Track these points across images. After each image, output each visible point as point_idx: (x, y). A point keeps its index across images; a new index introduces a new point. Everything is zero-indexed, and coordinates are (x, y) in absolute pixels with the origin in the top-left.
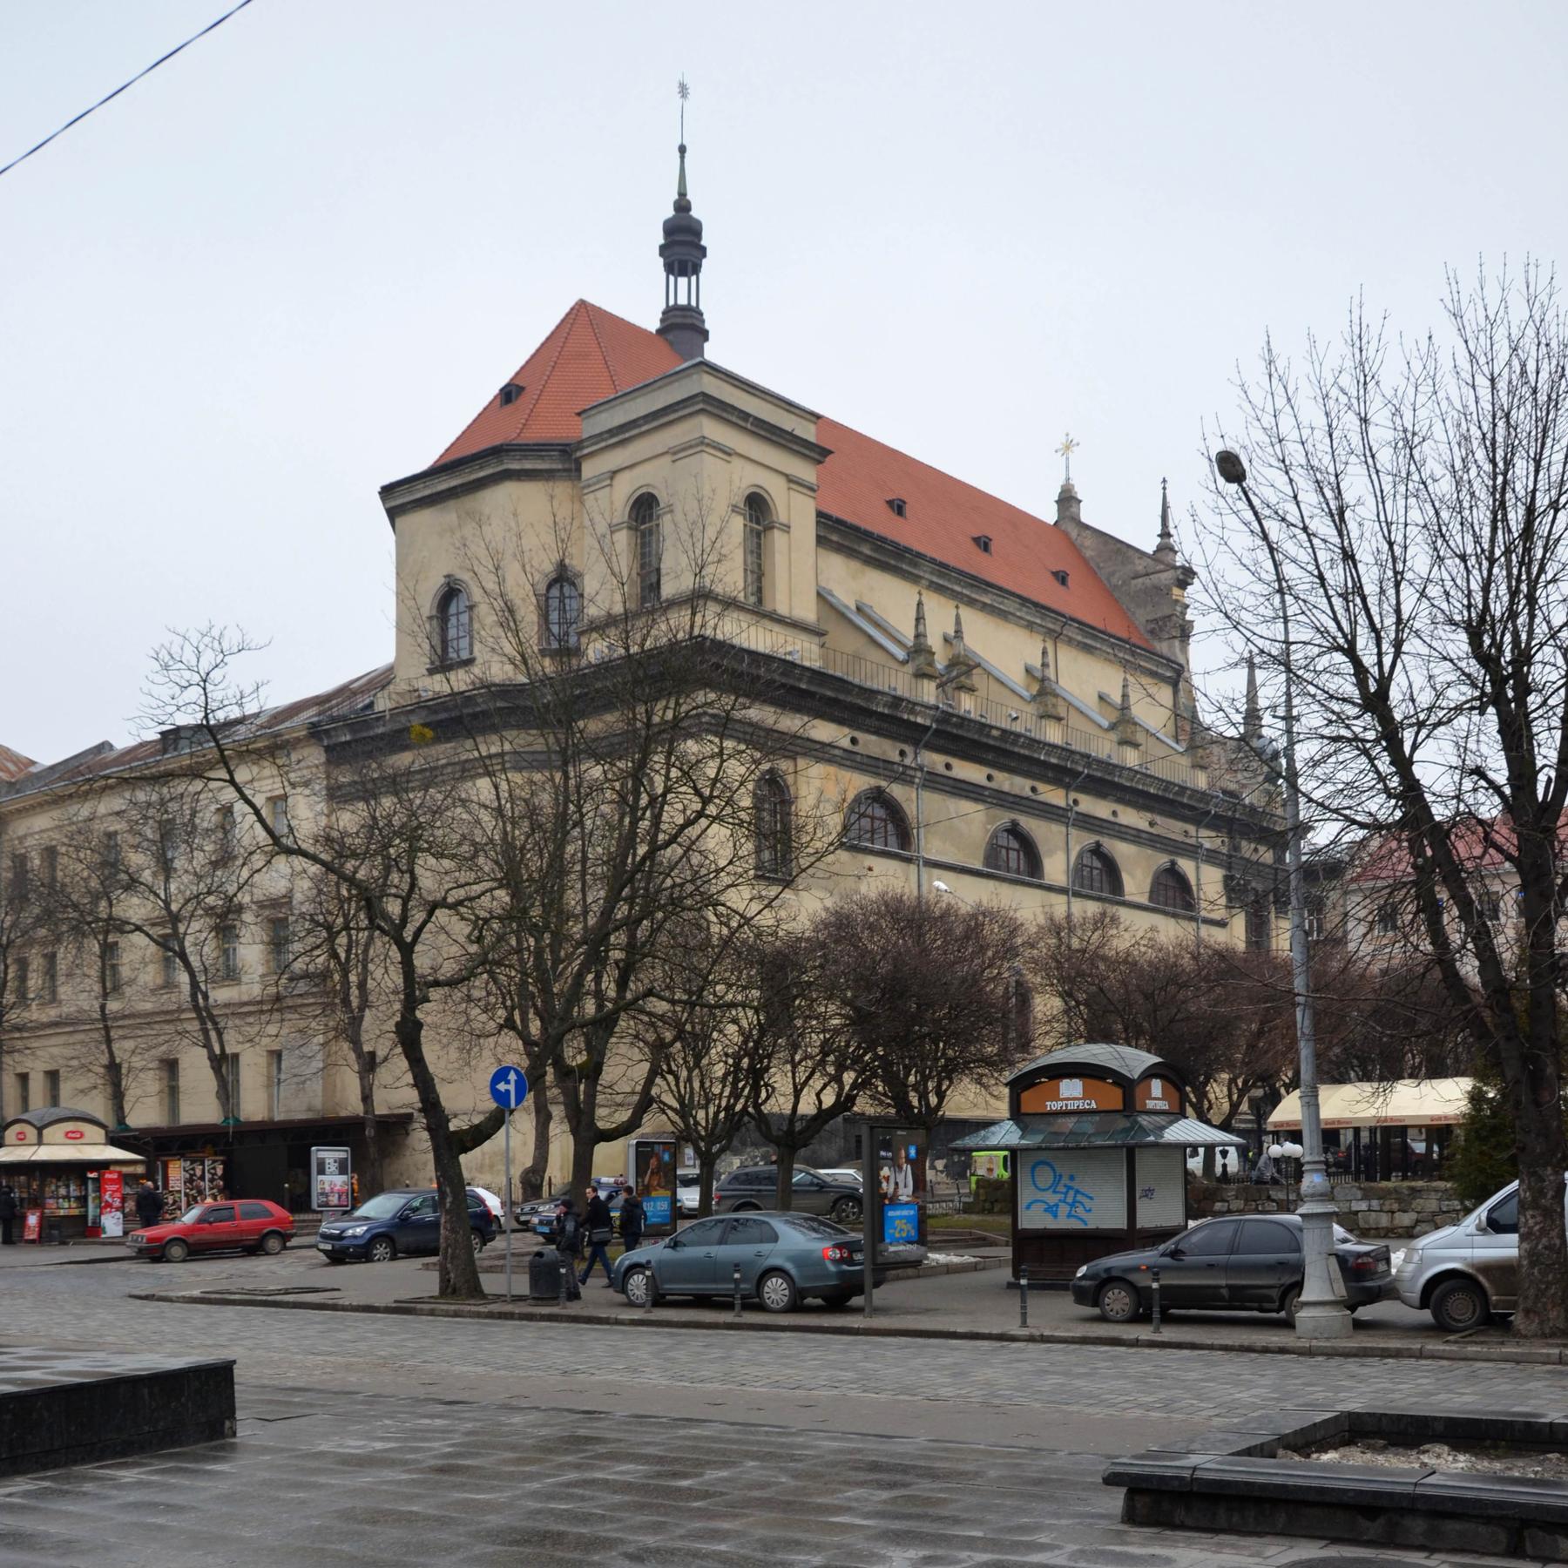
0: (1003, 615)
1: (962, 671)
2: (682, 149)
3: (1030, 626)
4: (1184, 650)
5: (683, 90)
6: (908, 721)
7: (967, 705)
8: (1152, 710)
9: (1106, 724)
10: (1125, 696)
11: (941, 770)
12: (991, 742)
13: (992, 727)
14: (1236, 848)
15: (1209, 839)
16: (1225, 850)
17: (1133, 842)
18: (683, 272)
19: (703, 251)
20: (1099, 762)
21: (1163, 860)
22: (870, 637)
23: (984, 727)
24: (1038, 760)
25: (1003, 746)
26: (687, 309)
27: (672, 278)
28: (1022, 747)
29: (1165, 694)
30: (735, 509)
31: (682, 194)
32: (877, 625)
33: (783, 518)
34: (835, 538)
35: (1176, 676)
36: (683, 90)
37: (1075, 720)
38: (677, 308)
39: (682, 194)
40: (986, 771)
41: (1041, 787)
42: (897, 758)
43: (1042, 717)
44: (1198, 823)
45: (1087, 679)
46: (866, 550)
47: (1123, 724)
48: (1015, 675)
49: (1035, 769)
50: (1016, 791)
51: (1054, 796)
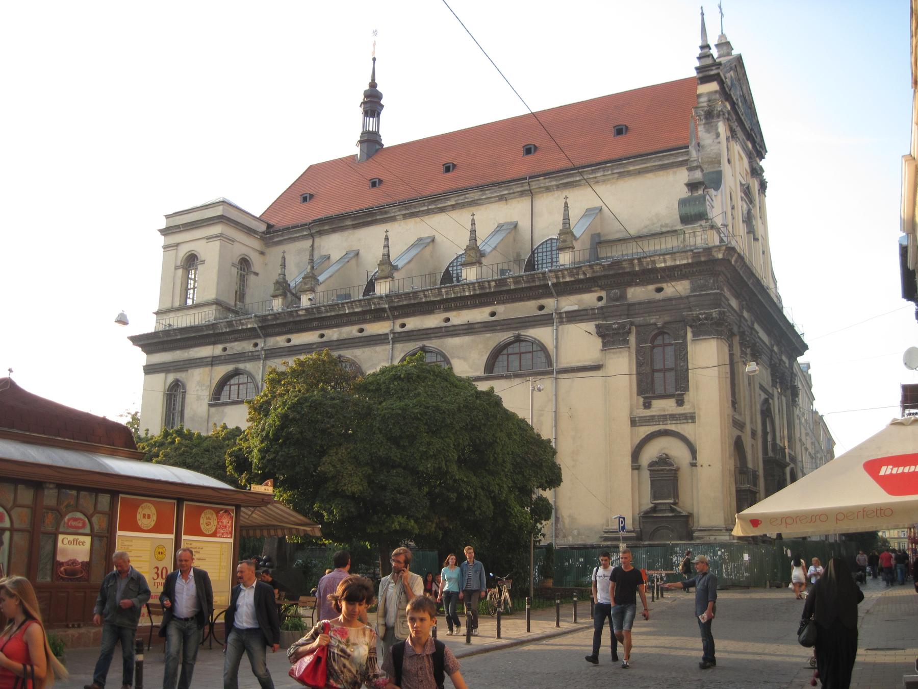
2: (374, 60)
5: (375, 33)
6: (242, 329)
12: (303, 318)
25: (313, 317)
28: (327, 311)
31: (373, 79)
34: (326, 227)
38: (369, 132)
39: (373, 79)
46: (349, 222)
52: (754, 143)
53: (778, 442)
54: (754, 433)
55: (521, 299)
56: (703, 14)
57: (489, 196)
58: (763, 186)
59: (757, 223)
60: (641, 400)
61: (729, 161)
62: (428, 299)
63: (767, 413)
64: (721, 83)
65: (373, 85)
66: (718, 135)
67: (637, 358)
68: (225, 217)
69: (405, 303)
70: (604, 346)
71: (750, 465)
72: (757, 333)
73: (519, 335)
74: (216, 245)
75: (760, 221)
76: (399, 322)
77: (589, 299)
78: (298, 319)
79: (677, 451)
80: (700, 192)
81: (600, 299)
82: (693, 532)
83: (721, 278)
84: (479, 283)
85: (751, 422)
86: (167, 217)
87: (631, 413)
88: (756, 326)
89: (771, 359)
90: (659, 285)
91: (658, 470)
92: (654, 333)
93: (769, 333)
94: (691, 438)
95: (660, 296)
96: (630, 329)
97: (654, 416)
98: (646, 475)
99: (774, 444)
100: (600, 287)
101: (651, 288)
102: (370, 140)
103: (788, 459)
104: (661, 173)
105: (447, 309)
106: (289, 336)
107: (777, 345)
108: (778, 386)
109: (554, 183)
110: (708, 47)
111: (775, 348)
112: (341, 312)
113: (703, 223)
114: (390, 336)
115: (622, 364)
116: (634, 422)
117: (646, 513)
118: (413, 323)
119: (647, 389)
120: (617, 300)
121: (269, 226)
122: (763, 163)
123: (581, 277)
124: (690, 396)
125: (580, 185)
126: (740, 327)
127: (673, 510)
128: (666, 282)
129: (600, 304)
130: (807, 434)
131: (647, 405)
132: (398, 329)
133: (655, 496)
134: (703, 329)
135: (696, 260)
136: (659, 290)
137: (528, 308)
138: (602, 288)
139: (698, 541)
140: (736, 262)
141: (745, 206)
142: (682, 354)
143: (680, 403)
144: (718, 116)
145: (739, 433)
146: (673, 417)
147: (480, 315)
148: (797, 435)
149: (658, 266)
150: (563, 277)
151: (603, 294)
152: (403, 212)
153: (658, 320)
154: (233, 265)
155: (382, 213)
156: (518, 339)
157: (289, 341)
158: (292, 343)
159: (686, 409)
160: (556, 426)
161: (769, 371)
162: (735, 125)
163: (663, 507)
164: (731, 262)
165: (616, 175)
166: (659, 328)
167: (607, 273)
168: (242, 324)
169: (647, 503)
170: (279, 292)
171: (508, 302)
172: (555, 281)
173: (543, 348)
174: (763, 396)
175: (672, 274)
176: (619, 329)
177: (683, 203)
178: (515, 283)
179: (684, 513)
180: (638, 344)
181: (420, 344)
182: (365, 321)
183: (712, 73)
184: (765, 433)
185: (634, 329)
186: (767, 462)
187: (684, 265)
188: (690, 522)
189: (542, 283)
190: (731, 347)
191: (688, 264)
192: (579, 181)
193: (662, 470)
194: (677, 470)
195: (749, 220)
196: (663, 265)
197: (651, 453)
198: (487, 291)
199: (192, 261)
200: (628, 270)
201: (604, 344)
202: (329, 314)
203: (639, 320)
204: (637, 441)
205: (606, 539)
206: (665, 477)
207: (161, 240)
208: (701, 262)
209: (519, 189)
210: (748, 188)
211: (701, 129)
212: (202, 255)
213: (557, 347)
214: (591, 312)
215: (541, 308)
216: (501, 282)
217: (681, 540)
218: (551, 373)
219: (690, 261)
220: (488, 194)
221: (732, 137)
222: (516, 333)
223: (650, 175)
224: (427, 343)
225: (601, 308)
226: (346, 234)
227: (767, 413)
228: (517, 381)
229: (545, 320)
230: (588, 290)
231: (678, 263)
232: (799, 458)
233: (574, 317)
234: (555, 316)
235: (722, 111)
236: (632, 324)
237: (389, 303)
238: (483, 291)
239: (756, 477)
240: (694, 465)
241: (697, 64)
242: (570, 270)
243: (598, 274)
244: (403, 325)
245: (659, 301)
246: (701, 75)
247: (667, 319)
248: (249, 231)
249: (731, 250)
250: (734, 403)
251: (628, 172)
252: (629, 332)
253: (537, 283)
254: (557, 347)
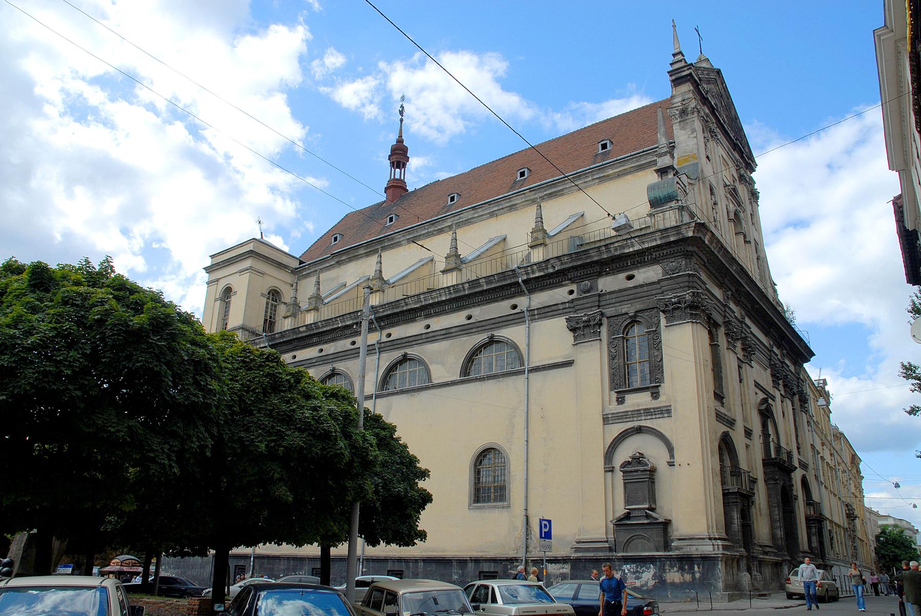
12: (304, 334)
18: (398, 167)
24: (338, 328)
25: (312, 333)
26: (400, 180)
28: (323, 327)
31: (401, 136)
34: (344, 258)
39: (401, 136)
46: (362, 251)
49: (302, 343)
52: (741, 154)
53: (783, 444)
54: (748, 433)
55: (495, 300)
56: (674, 26)
57: (481, 214)
58: (754, 195)
59: (746, 225)
60: (614, 396)
61: (708, 157)
62: (409, 307)
63: (766, 414)
64: (696, 85)
65: (400, 141)
66: (693, 131)
67: (609, 351)
68: (256, 253)
69: (389, 312)
70: (575, 341)
71: (743, 465)
72: (749, 328)
73: (493, 336)
74: (246, 276)
75: (752, 229)
77: (560, 294)
79: (654, 452)
80: (671, 176)
81: (571, 292)
82: (672, 541)
83: (694, 260)
84: (453, 286)
85: (745, 419)
86: (212, 257)
87: (603, 411)
88: (748, 321)
89: (770, 360)
90: (630, 273)
91: (631, 472)
92: (626, 323)
93: (767, 334)
94: (667, 434)
95: (631, 284)
96: (600, 320)
97: (627, 412)
98: (619, 475)
99: (778, 448)
100: (570, 279)
101: (622, 276)
102: (396, 188)
103: (796, 464)
104: (640, 174)
105: (428, 316)
106: (294, 353)
107: (778, 348)
108: (781, 387)
109: (541, 195)
110: (680, 53)
111: (775, 349)
113: (673, 204)
114: (377, 347)
115: (593, 359)
116: (606, 420)
117: (620, 520)
118: (398, 332)
119: (621, 383)
120: (588, 291)
121: (301, 262)
122: (753, 175)
123: (551, 271)
124: (665, 389)
125: (563, 195)
126: (725, 317)
127: (647, 516)
128: (637, 268)
129: (571, 297)
130: (823, 444)
131: (621, 401)
132: (384, 339)
133: (628, 501)
134: (675, 311)
135: (664, 241)
136: (630, 278)
137: (501, 308)
138: (573, 281)
139: (677, 552)
140: (711, 242)
141: (732, 206)
142: (654, 342)
143: (655, 396)
144: (693, 114)
145: (729, 430)
146: (648, 412)
147: (457, 319)
148: (809, 441)
149: (627, 251)
150: (533, 272)
151: (574, 287)
153: (629, 309)
154: (262, 295)
155: (389, 240)
156: (492, 341)
157: (294, 357)
158: (296, 360)
159: (662, 402)
160: (527, 428)
161: (769, 370)
162: (714, 126)
163: (637, 513)
164: (704, 242)
165: (597, 181)
166: (631, 317)
167: (575, 264)
168: (257, 344)
169: (621, 510)
170: (289, 314)
171: (483, 304)
172: (525, 277)
173: (515, 347)
174: (761, 396)
175: (641, 258)
176: (589, 321)
177: (651, 188)
178: (487, 283)
179: (660, 520)
180: (609, 335)
181: (402, 352)
183: (684, 74)
184: (766, 435)
185: (605, 320)
186: (768, 463)
187: (653, 247)
188: (669, 530)
189: (513, 281)
190: (712, 337)
191: (658, 246)
192: (563, 190)
193: (636, 471)
194: (653, 471)
195: (736, 219)
196: (631, 250)
197: (624, 454)
198: (462, 293)
199: (228, 291)
200: (596, 259)
201: (575, 338)
203: (609, 311)
204: (609, 440)
205: (577, 550)
206: (641, 478)
207: (206, 276)
208: (670, 243)
209: (507, 205)
210: (734, 189)
211: (676, 127)
212: (234, 289)
213: (528, 345)
214: (561, 307)
215: (515, 307)
216: (475, 283)
217: (657, 551)
218: (522, 372)
219: (659, 242)
220: (480, 212)
221: (712, 137)
222: (489, 334)
223: (629, 177)
224: (409, 351)
225: (572, 301)
226: (360, 262)
227: (766, 414)
228: (490, 384)
229: (516, 319)
230: (559, 285)
231: (646, 246)
232: (811, 466)
233: (547, 312)
234: (527, 314)
235: (696, 107)
236: (602, 314)
237: (375, 314)
238: (458, 295)
239: (754, 481)
240: (671, 464)
241: (670, 69)
242: (538, 264)
243: (567, 266)
244: (389, 335)
245: (630, 289)
246: (673, 78)
247: (639, 307)
248: (281, 266)
249: (701, 227)
250: (719, 397)
251: (608, 176)
252: (600, 324)
253: (509, 282)
254: (528, 345)
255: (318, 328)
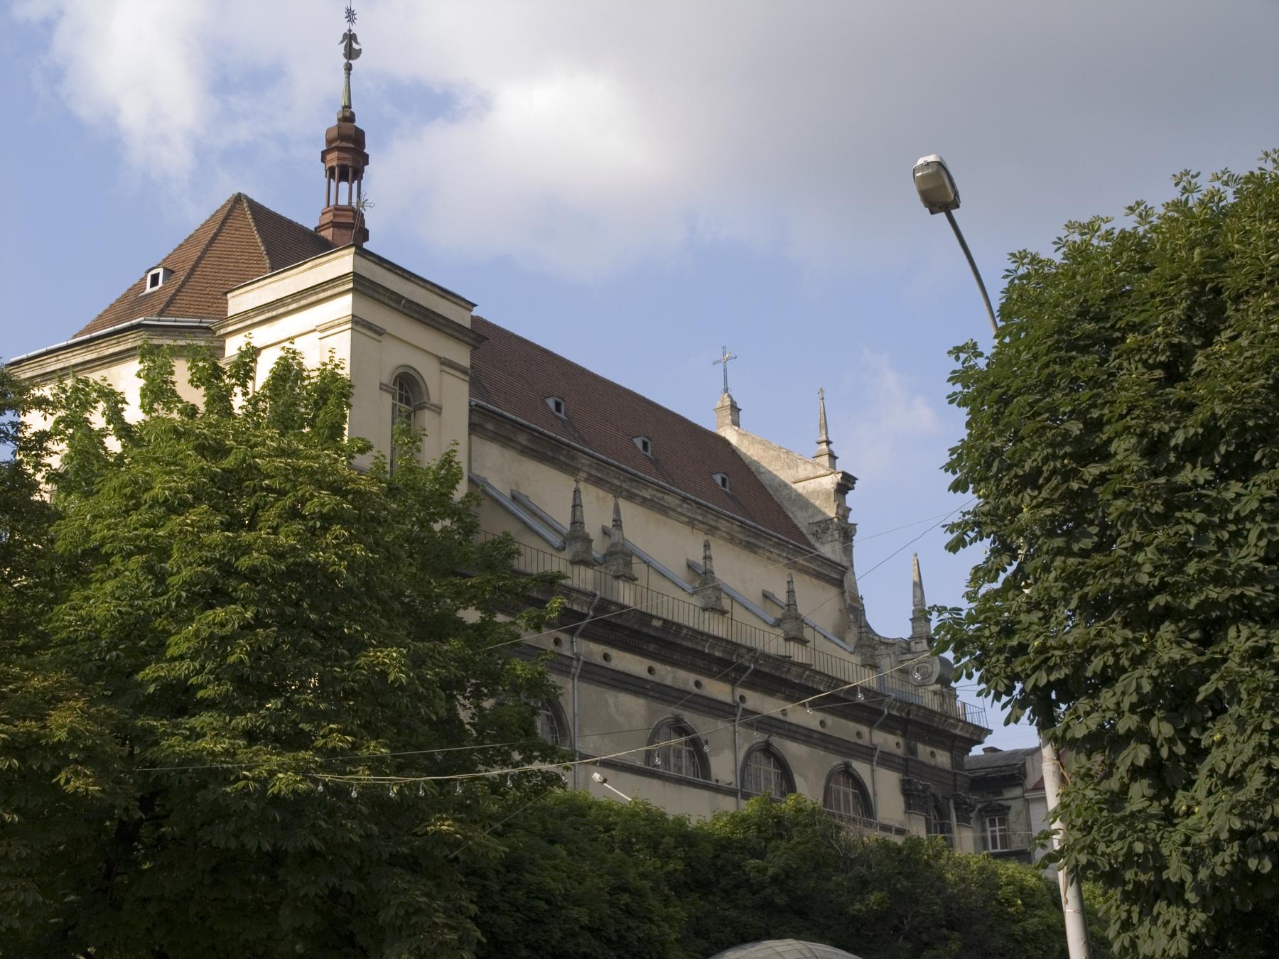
0: (664, 510)
1: (621, 559)
3: (691, 523)
4: (848, 550)
5: (351, 16)
7: (626, 595)
8: (817, 604)
9: (771, 620)
10: (791, 592)
11: (599, 660)
12: (653, 633)
13: (652, 617)
14: (912, 751)
15: (887, 741)
16: (900, 752)
17: (805, 742)
19: (367, 156)
20: (766, 657)
21: (836, 761)
22: (524, 523)
23: (645, 617)
24: (703, 653)
27: (333, 184)
28: (684, 638)
29: (833, 592)
30: (383, 387)
32: (534, 514)
33: (434, 399)
35: (837, 576)
36: (351, 16)
37: (739, 613)
40: (649, 663)
41: (705, 681)
42: (552, 647)
43: (704, 610)
44: (870, 724)
45: (749, 576)
46: (522, 439)
47: (791, 621)
48: (677, 568)
49: (700, 663)
50: (679, 685)
51: (718, 690)
69: (767, 670)
76: (740, 691)
78: (646, 630)
112: (699, 648)
125: (755, 553)
152: (594, 472)
182: (711, 675)
202: (685, 643)
255: (677, 633)
